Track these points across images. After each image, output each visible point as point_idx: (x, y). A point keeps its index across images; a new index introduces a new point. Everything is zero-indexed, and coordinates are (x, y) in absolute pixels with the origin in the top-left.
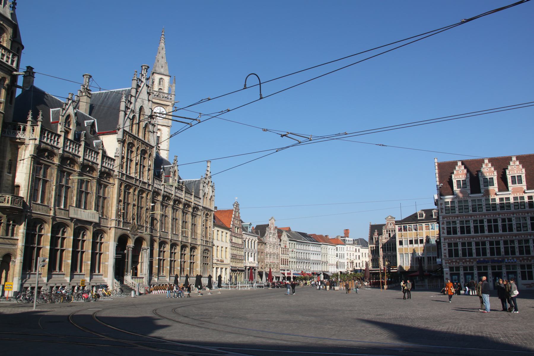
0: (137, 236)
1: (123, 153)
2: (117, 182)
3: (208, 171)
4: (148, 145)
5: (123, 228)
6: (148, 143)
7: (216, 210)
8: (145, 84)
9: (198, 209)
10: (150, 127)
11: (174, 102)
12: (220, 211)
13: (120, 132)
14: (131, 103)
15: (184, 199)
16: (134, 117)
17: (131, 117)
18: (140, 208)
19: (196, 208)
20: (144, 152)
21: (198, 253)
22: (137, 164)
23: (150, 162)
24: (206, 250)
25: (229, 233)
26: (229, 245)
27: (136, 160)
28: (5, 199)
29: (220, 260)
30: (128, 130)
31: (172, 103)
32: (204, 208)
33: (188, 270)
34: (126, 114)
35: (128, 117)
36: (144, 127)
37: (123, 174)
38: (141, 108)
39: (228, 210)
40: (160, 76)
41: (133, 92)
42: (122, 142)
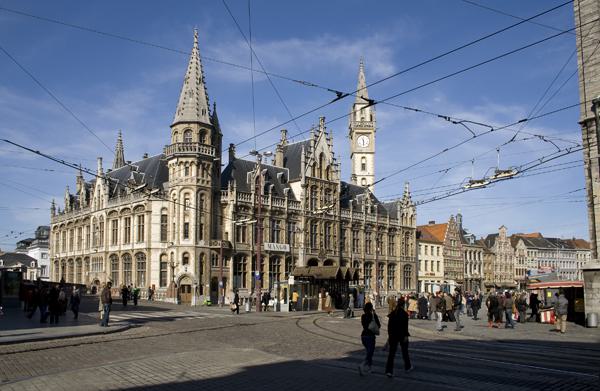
2: (303, 219)
4: (330, 184)
9: (396, 230)
10: (333, 168)
13: (303, 179)
16: (315, 164)
17: (312, 164)
18: (327, 237)
19: (392, 229)
20: (328, 191)
21: (398, 269)
26: (441, 259)
34: (306, 164)
37: (308, 212)
38: (322, 155)
41: (312, 143)
42: (305, 186)
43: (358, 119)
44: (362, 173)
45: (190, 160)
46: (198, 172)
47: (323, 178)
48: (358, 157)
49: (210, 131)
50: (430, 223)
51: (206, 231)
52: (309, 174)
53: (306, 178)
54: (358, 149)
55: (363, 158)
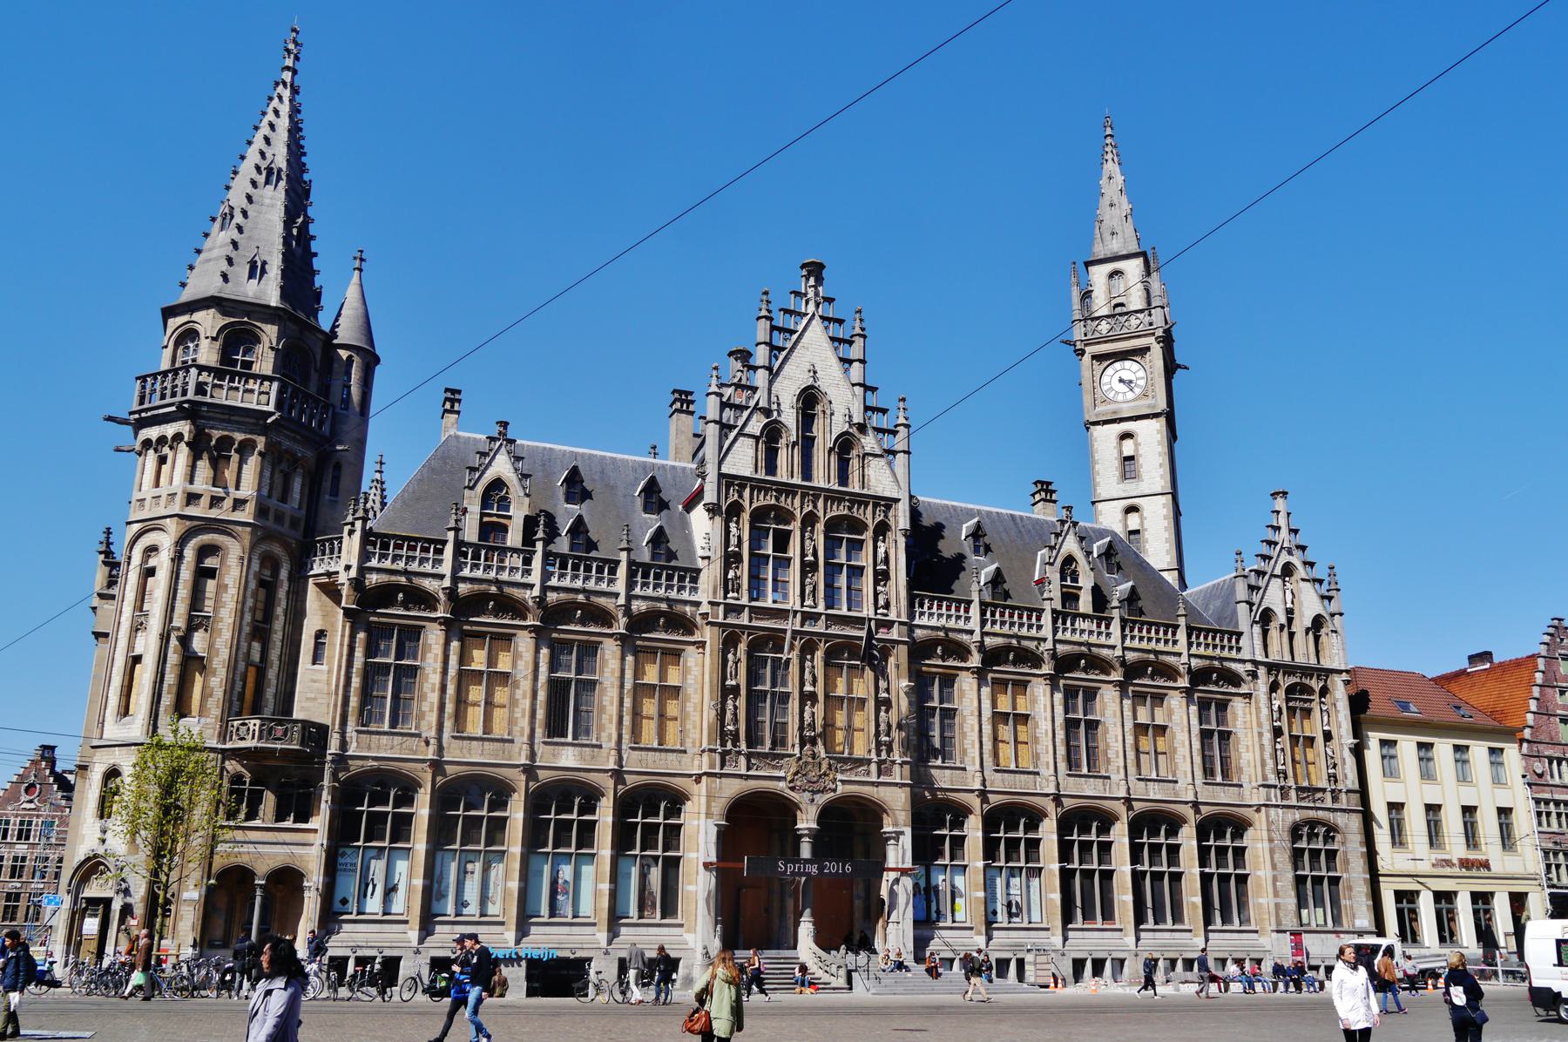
0: (831, 795)
1: (733, 541)
2: (708, 635)
3: (1277, 529)
4: (860, 500)
5: (750, 773)
6: (865, 491)
7: (1487, 666)
8: (817, 317)
11: (1161, 330)
12: (1501, 664)
14: (754, 389)
15: (1119, 647)
22: (808, 568)
23: (881, 551)
24: (1313, 824)
25: (1512, 753)
27: (803, 555)
28: (249, 729)
29: (1455, 861)
30: (746, 471)
31: (1157, 335)
32: (1272, 667)
33: (1194, 904)
35: (740, 434)
36: (831, 450)
37: (731, 609)
38: (809, 399)
39: (1528, 657)
40: (1110, 267)
43: (1101, 305)
44: (1130, 488)
45: (170, 430)
46: (193, 467)
47: (823, 477)
48: (1105, 437)
49: (270, 332)
50: (1473, 659)
51: (212, 687)
52: (743, 460)
53: (728, 481)
54: (1103, 411)
55: (1126, 436)
